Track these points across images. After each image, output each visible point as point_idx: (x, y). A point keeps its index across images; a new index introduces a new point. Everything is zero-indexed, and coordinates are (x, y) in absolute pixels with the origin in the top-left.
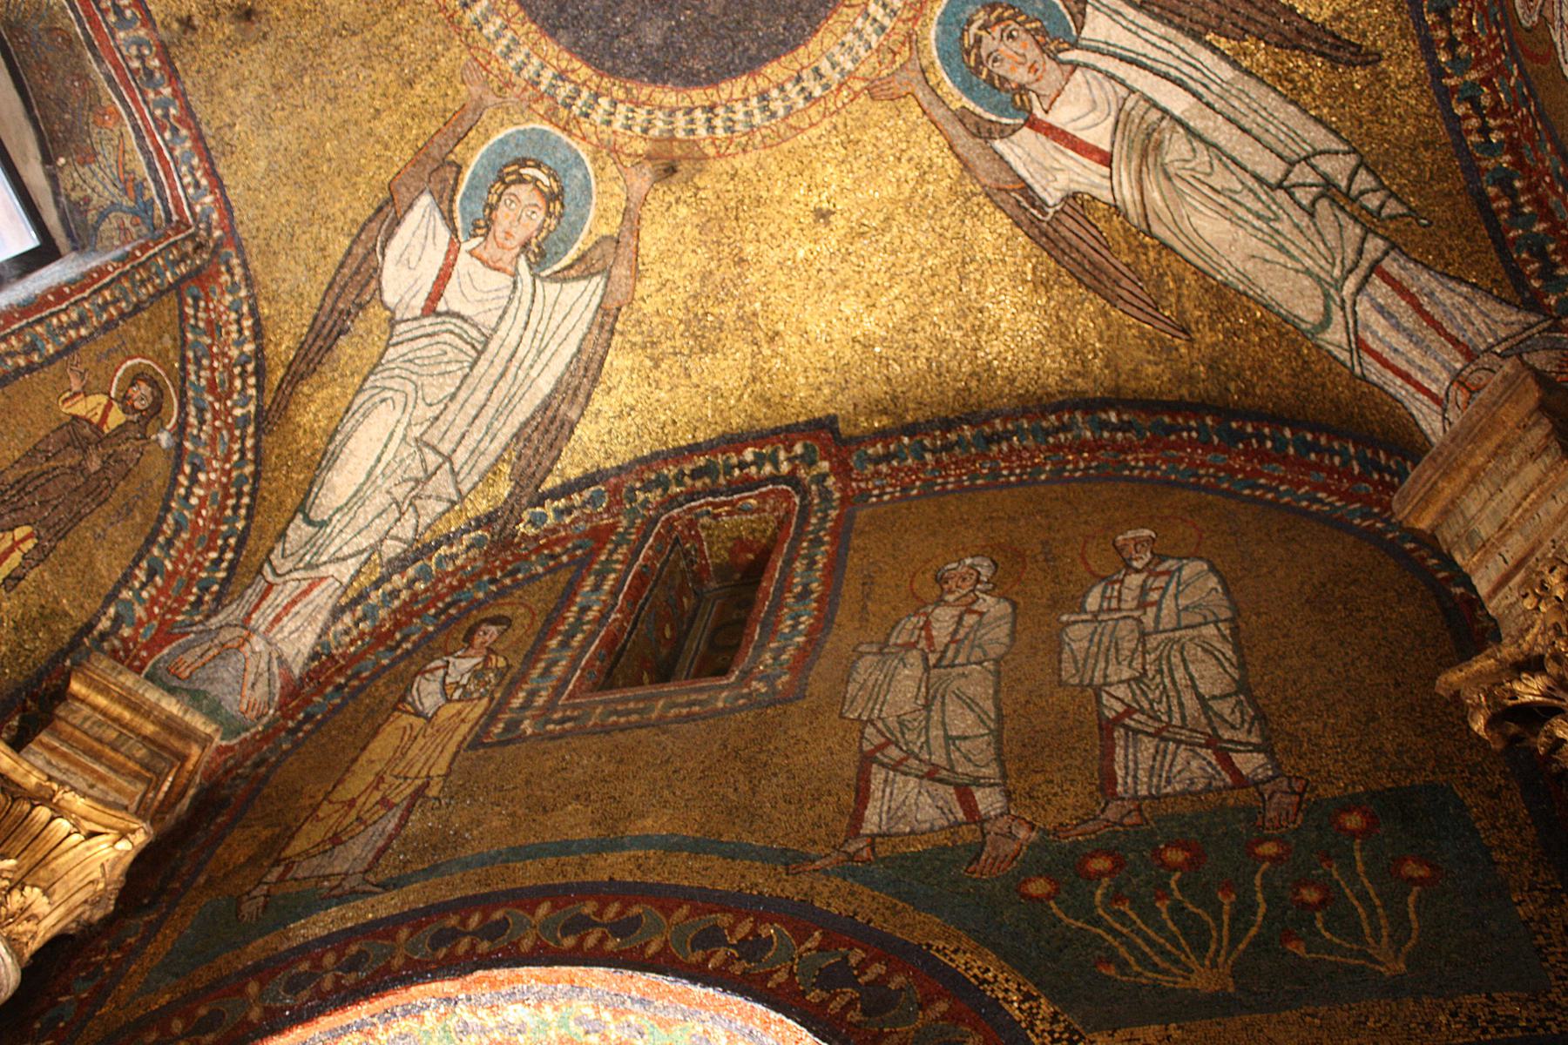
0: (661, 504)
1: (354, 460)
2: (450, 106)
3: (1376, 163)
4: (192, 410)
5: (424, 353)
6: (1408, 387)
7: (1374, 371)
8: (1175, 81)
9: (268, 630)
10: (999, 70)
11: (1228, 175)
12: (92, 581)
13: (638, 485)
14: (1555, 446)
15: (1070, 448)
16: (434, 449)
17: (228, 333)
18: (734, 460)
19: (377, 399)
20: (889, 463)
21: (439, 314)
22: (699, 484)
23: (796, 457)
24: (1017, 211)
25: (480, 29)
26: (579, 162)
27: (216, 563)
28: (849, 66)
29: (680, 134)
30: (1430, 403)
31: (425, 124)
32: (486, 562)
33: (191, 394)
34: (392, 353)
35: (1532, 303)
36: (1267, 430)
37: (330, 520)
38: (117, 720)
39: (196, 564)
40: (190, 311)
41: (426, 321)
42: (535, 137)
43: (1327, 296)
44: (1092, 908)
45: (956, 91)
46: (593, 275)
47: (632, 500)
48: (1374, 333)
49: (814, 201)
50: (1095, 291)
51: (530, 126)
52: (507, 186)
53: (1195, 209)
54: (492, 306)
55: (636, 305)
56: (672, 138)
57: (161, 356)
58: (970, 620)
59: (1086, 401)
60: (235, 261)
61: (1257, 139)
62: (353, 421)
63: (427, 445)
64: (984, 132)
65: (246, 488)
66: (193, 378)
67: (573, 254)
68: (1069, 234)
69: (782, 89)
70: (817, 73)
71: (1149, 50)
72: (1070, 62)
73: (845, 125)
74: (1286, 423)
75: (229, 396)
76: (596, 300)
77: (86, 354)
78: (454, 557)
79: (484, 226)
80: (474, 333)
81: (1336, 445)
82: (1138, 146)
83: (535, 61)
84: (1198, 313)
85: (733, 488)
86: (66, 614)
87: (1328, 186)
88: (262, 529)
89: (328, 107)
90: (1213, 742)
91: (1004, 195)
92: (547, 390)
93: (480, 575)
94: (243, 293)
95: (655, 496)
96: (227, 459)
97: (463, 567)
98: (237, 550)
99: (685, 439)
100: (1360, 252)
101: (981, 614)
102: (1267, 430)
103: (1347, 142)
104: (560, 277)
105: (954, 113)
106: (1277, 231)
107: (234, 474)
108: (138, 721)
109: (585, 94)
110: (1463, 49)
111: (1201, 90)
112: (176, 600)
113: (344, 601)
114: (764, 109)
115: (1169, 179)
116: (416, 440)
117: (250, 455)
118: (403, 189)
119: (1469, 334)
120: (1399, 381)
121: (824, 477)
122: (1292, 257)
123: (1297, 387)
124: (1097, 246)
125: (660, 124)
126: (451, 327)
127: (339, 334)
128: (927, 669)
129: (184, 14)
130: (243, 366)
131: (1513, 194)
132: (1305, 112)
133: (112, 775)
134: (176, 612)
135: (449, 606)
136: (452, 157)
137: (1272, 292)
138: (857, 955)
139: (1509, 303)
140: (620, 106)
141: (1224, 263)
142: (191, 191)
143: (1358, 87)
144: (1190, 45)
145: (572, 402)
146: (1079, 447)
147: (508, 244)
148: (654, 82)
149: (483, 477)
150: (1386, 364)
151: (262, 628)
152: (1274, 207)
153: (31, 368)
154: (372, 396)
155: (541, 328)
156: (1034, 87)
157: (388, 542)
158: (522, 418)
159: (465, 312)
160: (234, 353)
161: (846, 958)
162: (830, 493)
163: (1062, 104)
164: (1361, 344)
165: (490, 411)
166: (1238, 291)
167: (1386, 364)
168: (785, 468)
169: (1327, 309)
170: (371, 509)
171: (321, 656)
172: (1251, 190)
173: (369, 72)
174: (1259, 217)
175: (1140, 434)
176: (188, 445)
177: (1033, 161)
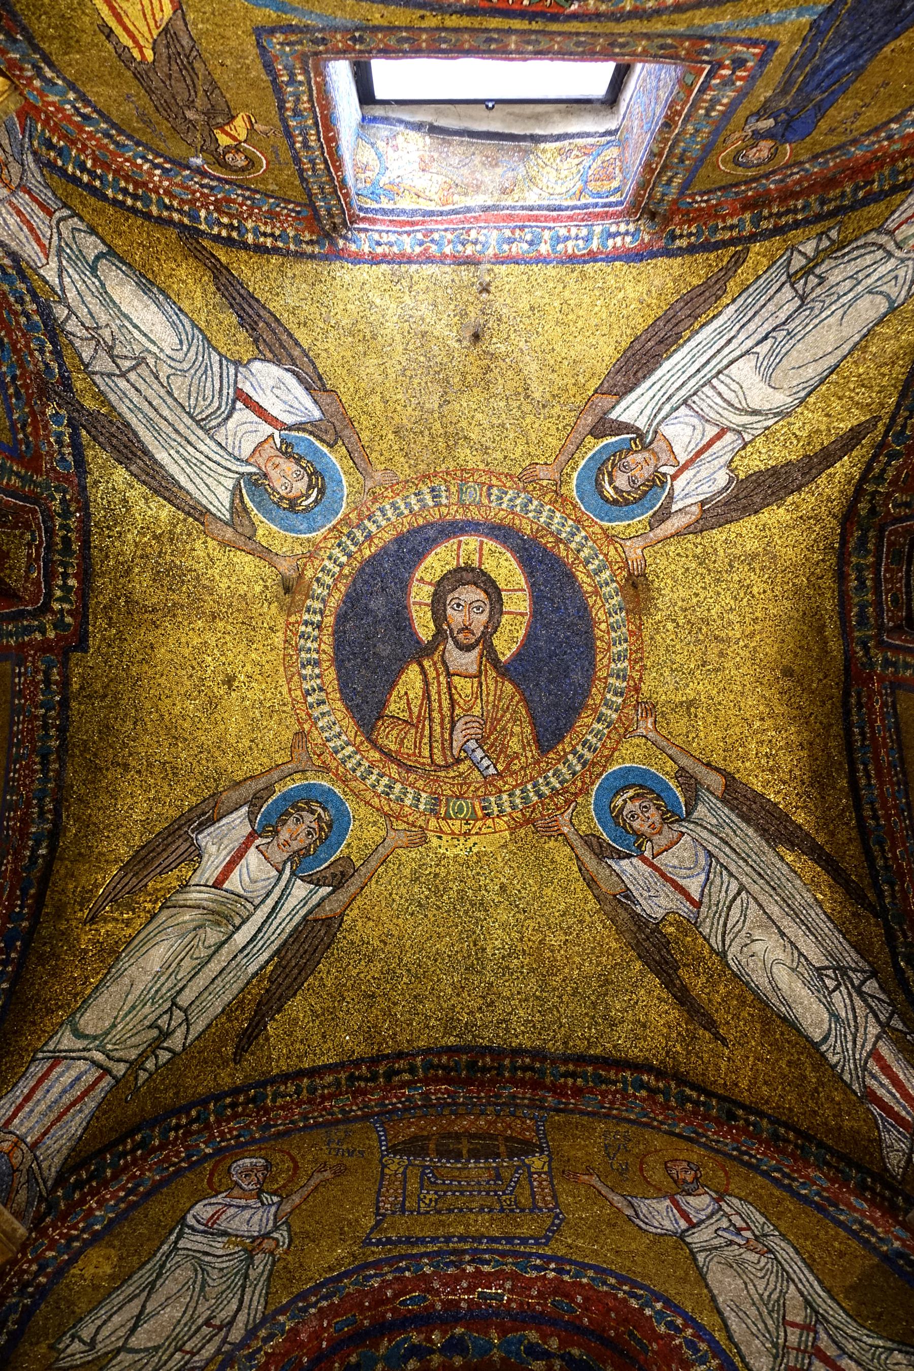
0: (49, 509)
1: (140, 306)
2: (374, 455)
5: (209, 384)
6: (21, 1099)
7: (37, 1069)
8: (255, 936)
9: (11, 203)
10: (291, 821)
12: (90, 80)
13: (68, 497)
15: (26, 814)
16: (133, 368)
17: (266, 224)
18: (70, 571)
19: (184, 337)
20: (43, 682)
21: (234, 402)
22: (58, 540)
23: (63, 616)
24: (199, 811)
25: (415, 494)
26: (311, 530)
27: (82, 167)
28: (320, 724)
29: (309, 602)
30: (7, 1117)
31: (368, 433)
32: (32, 373)
33: (227, 187)
34: (215, 358)
35: (60, 1179)
37: (97, 277)
39: (84, 145)
40: (291, 206)
41: (231, 391)
42: (336, 506)
43: (95, 1038)
45: (286, 789)
46: (232, 514)
47: (57, 489)
48: (62, 1074)
49: (242, 678)
50: (133, 857)
51: (344, 505)
52: (309, 476)
54: (230, 441)
56: (307, 597)
57: (263, 180)
59: (58, 834)
60: (317, 250)
62: (171, 313)
63: (138, 364)
64: (255, 802)
65: (139, 204)
66: (239, 192)
67: (250, 505)
68: (177, 844)
69: (318, 676)
70: (321, 703)
71: (278, 920)
72: (283, 869)
73: (284, 712)
74: (13, 985)
75: (217, 210)
76: (213, 510)
77: (282, 143)
78: (42, 351)
79: (287, 451)
80: (213, 423)
83: (384, 523)
84: (103, 931)
86: (66, 54)
87: (166, 1035)
88: (100, 212)
89: (399, 367)
92: (158, 456)
93: (21, 367)
94: (292, 247)
95: (56, 506)
96: (167, 192)
97: (32, 355)
98: (89, 187)
99: (95, 540)
100: (119, 1060)
103: (191, 1044)
104: (236, 491)
105: (272, 785)
107: (153, 196)
109: (353, 549)
110: (229, 1112)
111: (246, 952)
113: (24, 264)
114: (309, 663)
115: (195, 929)
116: (144, 358)
117: (165, 214)
118: (329, 401)
119: (48, 1142)
120: (26, 1091)
121: (43, 632)
122: (126, 1015)
123: (37, 1001)
125: (319, 591)
127: (239, 316)
129: (492, 289)
130: (237, 229)
131: (133, 1151)
132: (216, 1018)
134: (46, 123)
136: (340, 443)
137: (106, 995)
139: (64, 1164)
140: (338, 569)
141: (132, 961)
142: (376, 236)
144: (274, 947)
145: (143, 470)
146: (25, 821)
147: (270, 464)
148: (347, 595)
149: (101, 392)
150: (40, 1081)
151: (15, 201)
153: (281, 108)
155: (203, 467)
156: (275, 842)
157: (66, 312)
158: (141, 434)
159: (231, 424)
160: (250, 224)
163: (259, 859)
164: (57, 1061)
165: (152, 414)
166: (111, 967)
167: (40, 1081)
169: (86, 1037)
170: (96, 309)
173: (413, 406)
174: (157, 992)
175: (26, 869)
176: (188, 172)
177: (230, 830)
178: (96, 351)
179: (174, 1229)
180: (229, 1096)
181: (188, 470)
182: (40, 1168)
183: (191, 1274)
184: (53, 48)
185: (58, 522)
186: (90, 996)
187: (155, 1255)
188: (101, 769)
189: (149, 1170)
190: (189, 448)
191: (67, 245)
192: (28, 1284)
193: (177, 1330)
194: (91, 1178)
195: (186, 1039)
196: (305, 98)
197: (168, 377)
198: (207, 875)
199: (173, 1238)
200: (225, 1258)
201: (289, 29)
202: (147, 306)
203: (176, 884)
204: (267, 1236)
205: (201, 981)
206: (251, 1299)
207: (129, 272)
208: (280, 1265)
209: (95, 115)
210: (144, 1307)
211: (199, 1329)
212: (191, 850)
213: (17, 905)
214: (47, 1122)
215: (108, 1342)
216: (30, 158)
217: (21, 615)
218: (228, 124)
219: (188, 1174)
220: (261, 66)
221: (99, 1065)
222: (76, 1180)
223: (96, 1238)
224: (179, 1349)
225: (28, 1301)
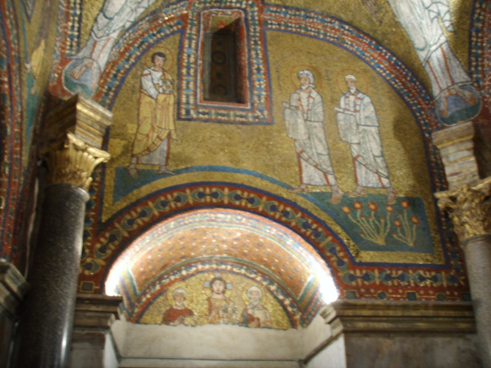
7: (428, 69)
22: (216, 5)
23: (248, 4)
27: (73, 27)
35: (470, 74)
38: (90, 117)
78: (142, 25)
90: (377, 172)
95: (201, 6)
100: (439, 39)
101: (314, 99)
135: (142, 43)
167: (432, 71)
171: (108, 63)
174: (419, 16)
175: (352, 34)
185: (208, 5)
194: (477, 61)
214: (447, 75)
221: (437, 49)
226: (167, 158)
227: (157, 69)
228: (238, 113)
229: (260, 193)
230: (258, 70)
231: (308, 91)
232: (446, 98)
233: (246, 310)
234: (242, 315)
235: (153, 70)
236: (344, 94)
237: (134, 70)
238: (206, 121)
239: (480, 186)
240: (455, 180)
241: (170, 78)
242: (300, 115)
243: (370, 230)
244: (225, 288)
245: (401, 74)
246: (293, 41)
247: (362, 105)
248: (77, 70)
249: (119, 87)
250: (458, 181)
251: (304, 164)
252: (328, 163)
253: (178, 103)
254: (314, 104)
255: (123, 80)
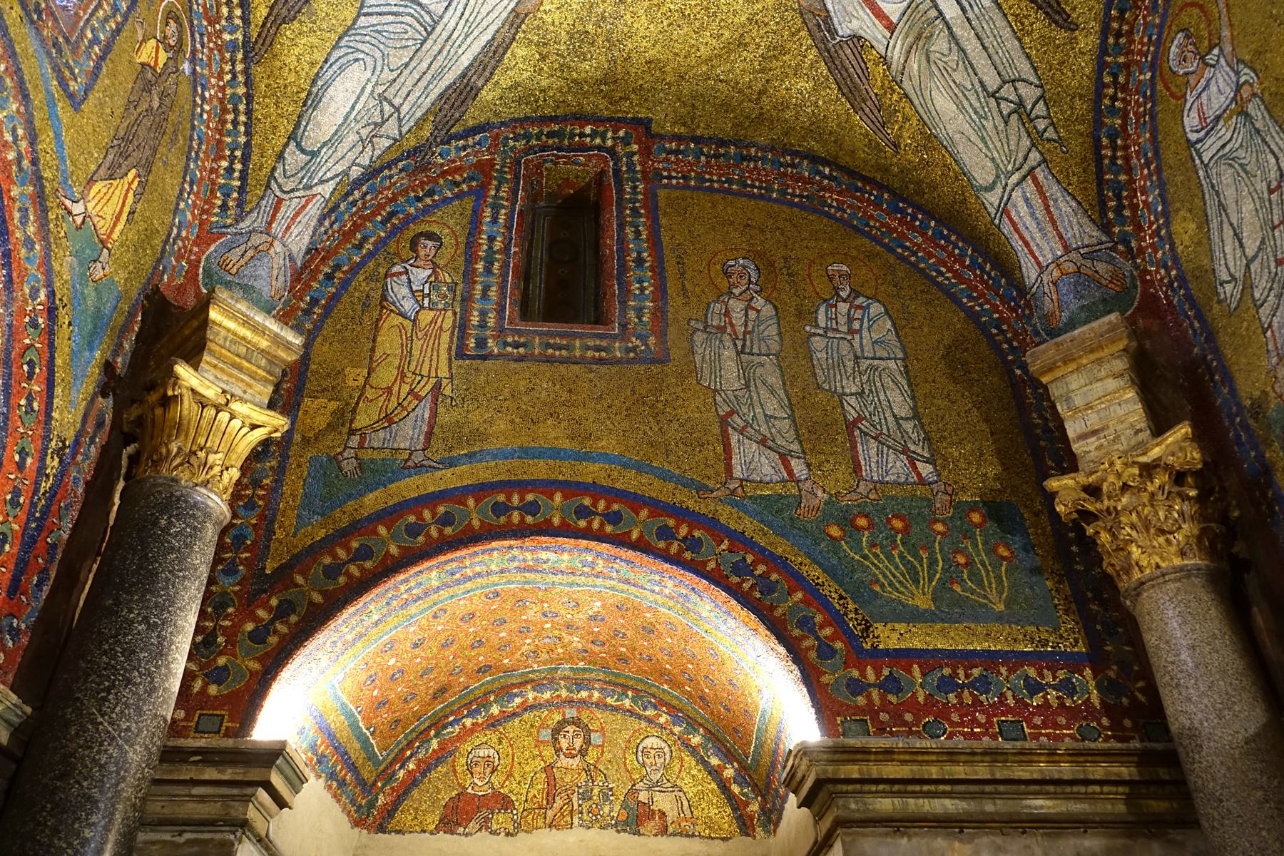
3: (1050, 99)
4: (197, 36)
5: (391, 28)
7: (1007, 228)
9: (283, 237)
11: (966, 76)
13: (511, 136)
14: (1127, 377)
15: (791, 177)
16: (392, 105)
19: (351, 57)
22: (550, 142)
23: (618, 138)
27: (230, 170)
30: (1035, 264)
33: (195, 22)
34: (363, 21)
35: (1105, 228)
36: (920, 216)
37: (319, 151)
38: (244, 338)
43: (998, 177)
44: (862, 549)
48: (1018, 213)
53: (938, 88)
55: (539, 15)
58: (752, 315)
61: (990, 57)
62: (331, 72)
63: (386, 99)
68: (844, 58)
74: (934, 219)
76: (512, 5)
78: (391, 177)
80: (428, 19)
81: (960, 244)
82: (915, 31)
85: (571, 149)
86: (158, 231)
90: (905, 451)
91: (811, 17)
92: (466, 64)
95: (520, 145)
97: (395, 183)
100: (1026, 158)
101: (758, 311)
102: (920, 216)
103: (1040, 79)
106: (984, 126)
107: (229, 91)
108: (256, 339)
110: (1122, 41)
111: (968, 7)
112: (206, 202)
113: (326, 210)
115: (928, 61)
116: (379, 95)
119: (1069, 235)
120: (1020, 243)
121: (633, 154)
124: (861, 74)
126: (412, 11)
128: (738, 354)
131: (1115, 148)
132: (1023, 48)
133: (252, 382)
135: (392, 214)
138: (750, 558)
141: (941, 126)
143: (1057, 42)
149: (416, 124)
150: (1017, 230)
151: (280, 235)
152: (986, 109)
154: (347, 54)
155: (471, 19)
158: (447, 83)
161: (744, 559)
162: (634, 165)
164: (1006, 212)
165: (428, 76)
167: (1017, 230)
168: (609, 143)
170: (346, 144)
171: (311, 251)
172: (976, 92)
174: (976, 112)
175: (839, 184)
178: (381, 137)
179: (1191, 155)
180: (1108, 38)
181: (476, 33)
182: (1087, 246)
183: (1230, 171)
184: (158, 242)
185: (534, 142)
186: (961, 168)
187: (1202, 185)
188: (761, 114)
189: (1139, 137)
190: (454, 36)
191: (300, 183)
192: (1171, 284)
193: (1261, 216)
194: (1118, 197)
195: (1031, 84)
196: (101, 12)
197: (392, 71)
198: (880, 37)
199: (1198, 162)
200: (1235, 135)
201: (63, 83)
202: (331, 98)
203: (881, 68)
204: (1239, 88)
205: (981, 61)
206: (1277, 143)
207: (306, 117)
208: (1266, 96)
209: (188, 179)
210: (1231, 224)
211: (1270, 200)
212: (851, 45)
213: (869, 198)
215: (1238, 268)
216: (242, 225)
217: (617, 172)
218: (149, 65)
219: (1158, 108)
220: (99, 81)
221: (1024, 177)
222: (1114, 212)
223: (1165, 214)
224: (1274, 228)
225: (1182, 292)
226: (429, 434)
227: (421, 263)
228: (591, 343)
229: (635, 501)
230: (640, 261)
231: (747, 295)
232: (1055, 284)
233: (633, 791)
234: (624, 806)
235: (411, 265)
236: (825, 301)
237: (371, 264)
238: (520, 359)
239: (1156, 452)
240: (1092, 448)
241: (449, 280)
242: (728, 343)
243: (894, 576)
244: (587, 742)
245: (951, 254)
246: (714, 206)
247: (866, 320)
248: (234, 256)
249: (335, 298)
250: (1098, 448)
251: (734, 438)
252: (791, 435)
253: (462, 327)
254: (758, 321)
255: (345, 284)
